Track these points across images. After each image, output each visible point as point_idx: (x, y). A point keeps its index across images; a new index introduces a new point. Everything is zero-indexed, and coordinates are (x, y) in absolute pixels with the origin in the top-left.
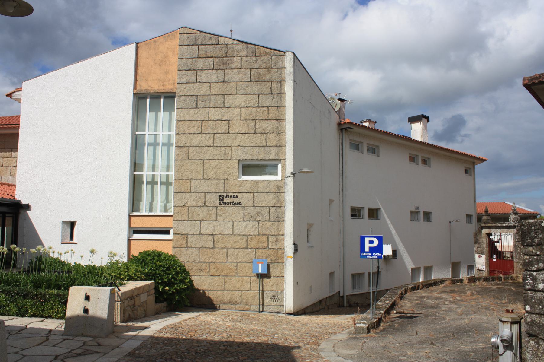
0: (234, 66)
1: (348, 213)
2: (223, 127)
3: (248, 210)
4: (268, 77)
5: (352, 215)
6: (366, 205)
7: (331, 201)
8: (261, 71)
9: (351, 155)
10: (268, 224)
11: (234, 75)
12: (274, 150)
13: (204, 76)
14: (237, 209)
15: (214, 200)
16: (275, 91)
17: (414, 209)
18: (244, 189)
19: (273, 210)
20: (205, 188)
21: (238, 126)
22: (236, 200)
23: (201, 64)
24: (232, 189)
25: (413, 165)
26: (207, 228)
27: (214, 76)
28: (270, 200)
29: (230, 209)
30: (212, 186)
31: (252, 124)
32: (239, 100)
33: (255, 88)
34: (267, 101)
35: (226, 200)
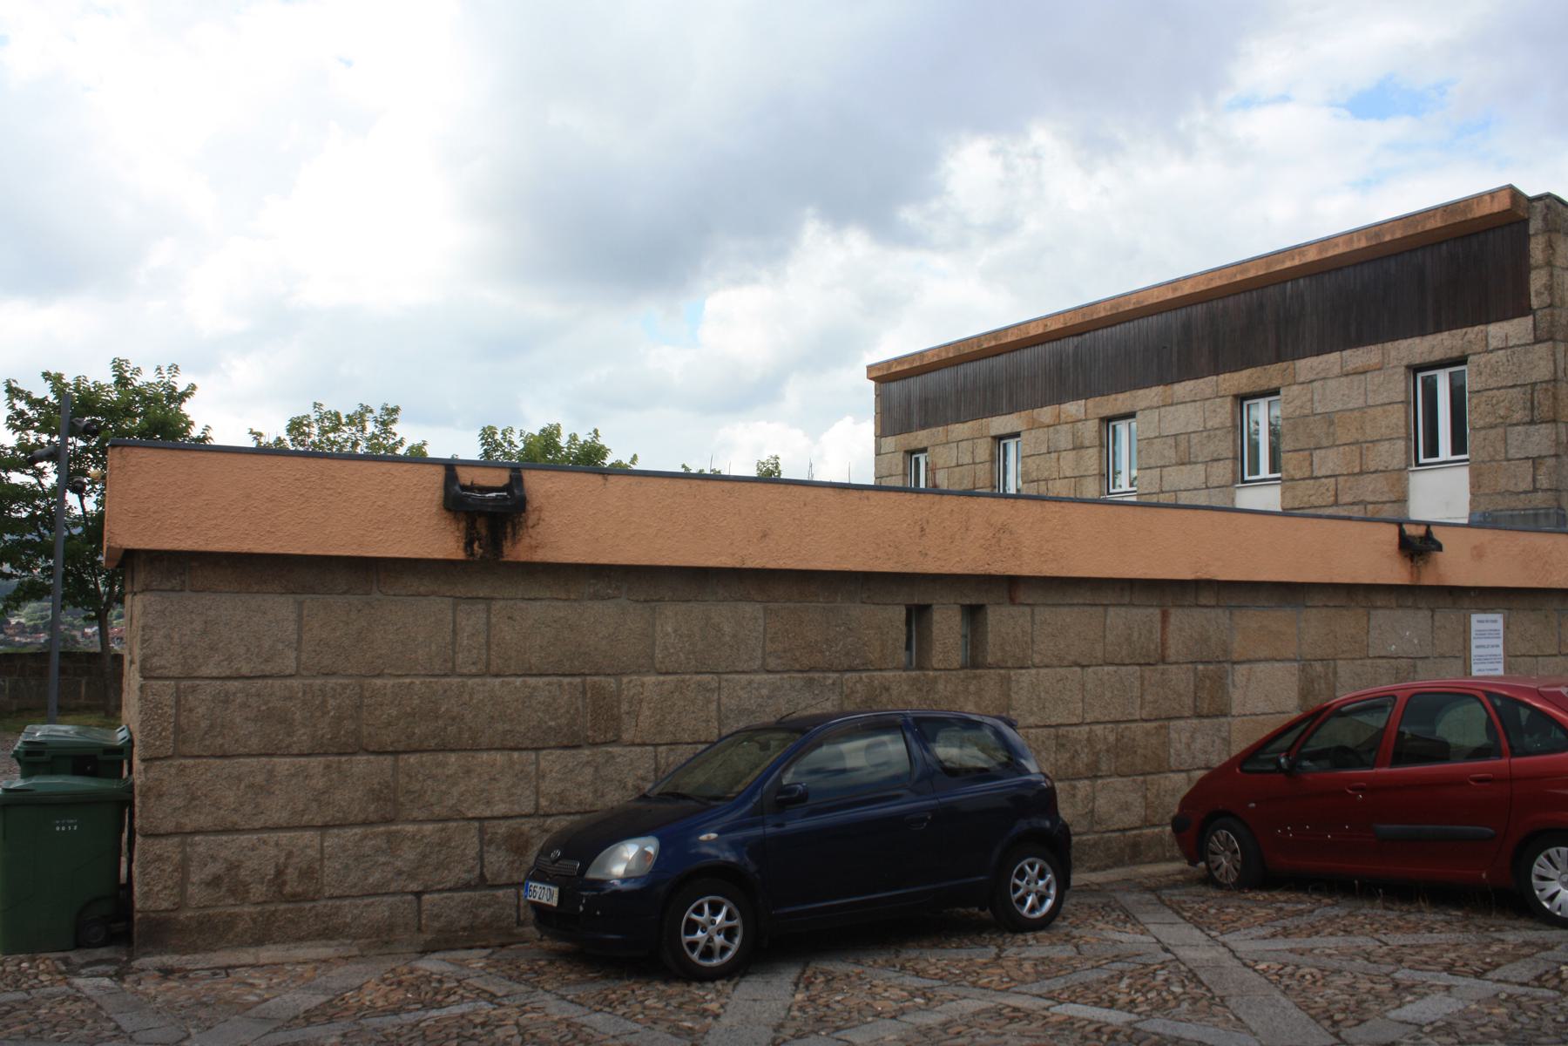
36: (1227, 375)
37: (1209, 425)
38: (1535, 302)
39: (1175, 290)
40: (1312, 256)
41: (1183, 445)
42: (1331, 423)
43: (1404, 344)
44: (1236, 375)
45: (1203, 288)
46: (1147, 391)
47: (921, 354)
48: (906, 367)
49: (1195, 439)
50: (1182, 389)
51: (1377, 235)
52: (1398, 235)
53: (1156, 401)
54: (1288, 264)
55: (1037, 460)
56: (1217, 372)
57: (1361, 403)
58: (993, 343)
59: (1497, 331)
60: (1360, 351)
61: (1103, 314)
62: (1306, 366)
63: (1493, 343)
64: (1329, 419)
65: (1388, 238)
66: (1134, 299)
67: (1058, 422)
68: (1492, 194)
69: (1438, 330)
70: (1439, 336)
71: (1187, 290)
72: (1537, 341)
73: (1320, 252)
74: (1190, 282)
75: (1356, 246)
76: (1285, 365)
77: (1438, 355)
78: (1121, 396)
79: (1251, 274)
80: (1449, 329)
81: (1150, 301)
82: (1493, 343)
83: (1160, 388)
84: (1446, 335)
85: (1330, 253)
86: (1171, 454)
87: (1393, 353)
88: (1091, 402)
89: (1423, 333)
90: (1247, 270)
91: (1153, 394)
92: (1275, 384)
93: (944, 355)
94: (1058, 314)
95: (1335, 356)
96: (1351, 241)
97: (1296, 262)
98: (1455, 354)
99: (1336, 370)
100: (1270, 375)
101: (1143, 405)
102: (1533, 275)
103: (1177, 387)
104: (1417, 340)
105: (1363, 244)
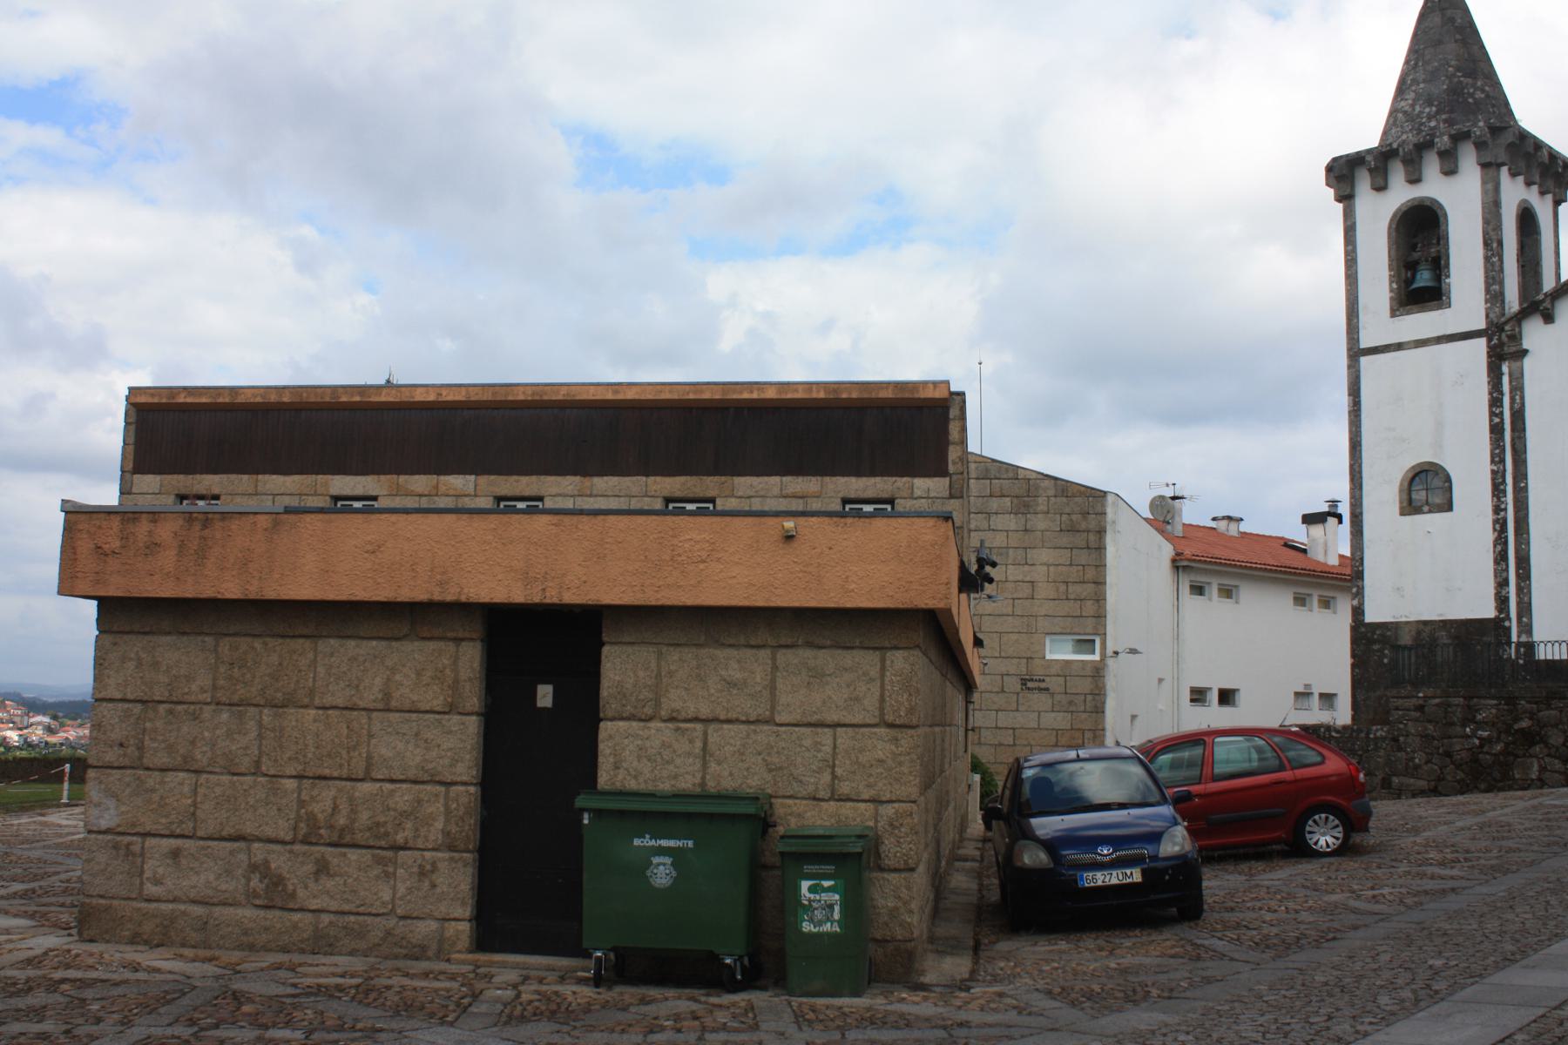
0: (1040, 508)
1: (1187, 695)
2: (1025, 590)
3: (1057, 698)
4: (1083, 526)
5: (1192, 700)
6: (1216, 684)
7: (1160, 680)
8: (1074, 517)
9: (1191, 602)
10: (1084, 716)
11: (1040, 523)
12: (1090, 621)
13: (999, 522)
14: (1044, 697)
15: (1013, 684)
16: (1092, 545)
17: (1301, 689)
18: (1053, 671)
19: (1089, 698)
20: (1004, 670)
21: (1044, 590)
22: (1043, 685)
23: (994, 504)
24: (1039, 671)
25: (1301, 612)
26: (1004, 720)
27: (1012, 522)
28: (1085, 685)
29: (1036, 696)
30: (1010, 667)
31: (1063, 588)
32: (1045, 555)
33: (1065, 540)
34: (1083, 557)
35: (1030, 684)
36: (658, 479)
38: (951, 469)
39: (616, 392)
40: (771, 394)
43: (841, 480)
45: (650, 397)
46: (559, 479)
47: (234, 390)
48: (204, 400)
51: (835, 391)
52: (854, 395)
53: (570, 489)
54: (746, 396)
58: (357, 399)
59: (921, 484)
60: (800, 479)
61: (521, 397)
63: (918, 493)
65: (844, 396)
66: (564, 391)
68: (935, 384)
69: (873, 474)
70: (873, 480)
71: (630, 395)
72: (951, 497)
73: (779, 392)
74: (634, 389)
75: (815, 395)
76: (723, 478)
77: (870, 494)
78: (524, 479)
79: (707, 396)
80: (882, 475)
81: (584, 397)
82: (918, 493)
84: (878, 479)
85: (789, 396)
87: (831, 486)
88: (483, 479)
89: (858, 474)
90: (702, 392)
92: (710, 494)
93: (273, 398)
94: (460, 386)
95: (775, 480)
96: (810, 390)
97: (755, 396)
98: (885, 495)
99: (776, 491)
101: (554, 490)
102: (951, 448)
103: (596, 480)
104: (853, 479)
105: (822, 395)
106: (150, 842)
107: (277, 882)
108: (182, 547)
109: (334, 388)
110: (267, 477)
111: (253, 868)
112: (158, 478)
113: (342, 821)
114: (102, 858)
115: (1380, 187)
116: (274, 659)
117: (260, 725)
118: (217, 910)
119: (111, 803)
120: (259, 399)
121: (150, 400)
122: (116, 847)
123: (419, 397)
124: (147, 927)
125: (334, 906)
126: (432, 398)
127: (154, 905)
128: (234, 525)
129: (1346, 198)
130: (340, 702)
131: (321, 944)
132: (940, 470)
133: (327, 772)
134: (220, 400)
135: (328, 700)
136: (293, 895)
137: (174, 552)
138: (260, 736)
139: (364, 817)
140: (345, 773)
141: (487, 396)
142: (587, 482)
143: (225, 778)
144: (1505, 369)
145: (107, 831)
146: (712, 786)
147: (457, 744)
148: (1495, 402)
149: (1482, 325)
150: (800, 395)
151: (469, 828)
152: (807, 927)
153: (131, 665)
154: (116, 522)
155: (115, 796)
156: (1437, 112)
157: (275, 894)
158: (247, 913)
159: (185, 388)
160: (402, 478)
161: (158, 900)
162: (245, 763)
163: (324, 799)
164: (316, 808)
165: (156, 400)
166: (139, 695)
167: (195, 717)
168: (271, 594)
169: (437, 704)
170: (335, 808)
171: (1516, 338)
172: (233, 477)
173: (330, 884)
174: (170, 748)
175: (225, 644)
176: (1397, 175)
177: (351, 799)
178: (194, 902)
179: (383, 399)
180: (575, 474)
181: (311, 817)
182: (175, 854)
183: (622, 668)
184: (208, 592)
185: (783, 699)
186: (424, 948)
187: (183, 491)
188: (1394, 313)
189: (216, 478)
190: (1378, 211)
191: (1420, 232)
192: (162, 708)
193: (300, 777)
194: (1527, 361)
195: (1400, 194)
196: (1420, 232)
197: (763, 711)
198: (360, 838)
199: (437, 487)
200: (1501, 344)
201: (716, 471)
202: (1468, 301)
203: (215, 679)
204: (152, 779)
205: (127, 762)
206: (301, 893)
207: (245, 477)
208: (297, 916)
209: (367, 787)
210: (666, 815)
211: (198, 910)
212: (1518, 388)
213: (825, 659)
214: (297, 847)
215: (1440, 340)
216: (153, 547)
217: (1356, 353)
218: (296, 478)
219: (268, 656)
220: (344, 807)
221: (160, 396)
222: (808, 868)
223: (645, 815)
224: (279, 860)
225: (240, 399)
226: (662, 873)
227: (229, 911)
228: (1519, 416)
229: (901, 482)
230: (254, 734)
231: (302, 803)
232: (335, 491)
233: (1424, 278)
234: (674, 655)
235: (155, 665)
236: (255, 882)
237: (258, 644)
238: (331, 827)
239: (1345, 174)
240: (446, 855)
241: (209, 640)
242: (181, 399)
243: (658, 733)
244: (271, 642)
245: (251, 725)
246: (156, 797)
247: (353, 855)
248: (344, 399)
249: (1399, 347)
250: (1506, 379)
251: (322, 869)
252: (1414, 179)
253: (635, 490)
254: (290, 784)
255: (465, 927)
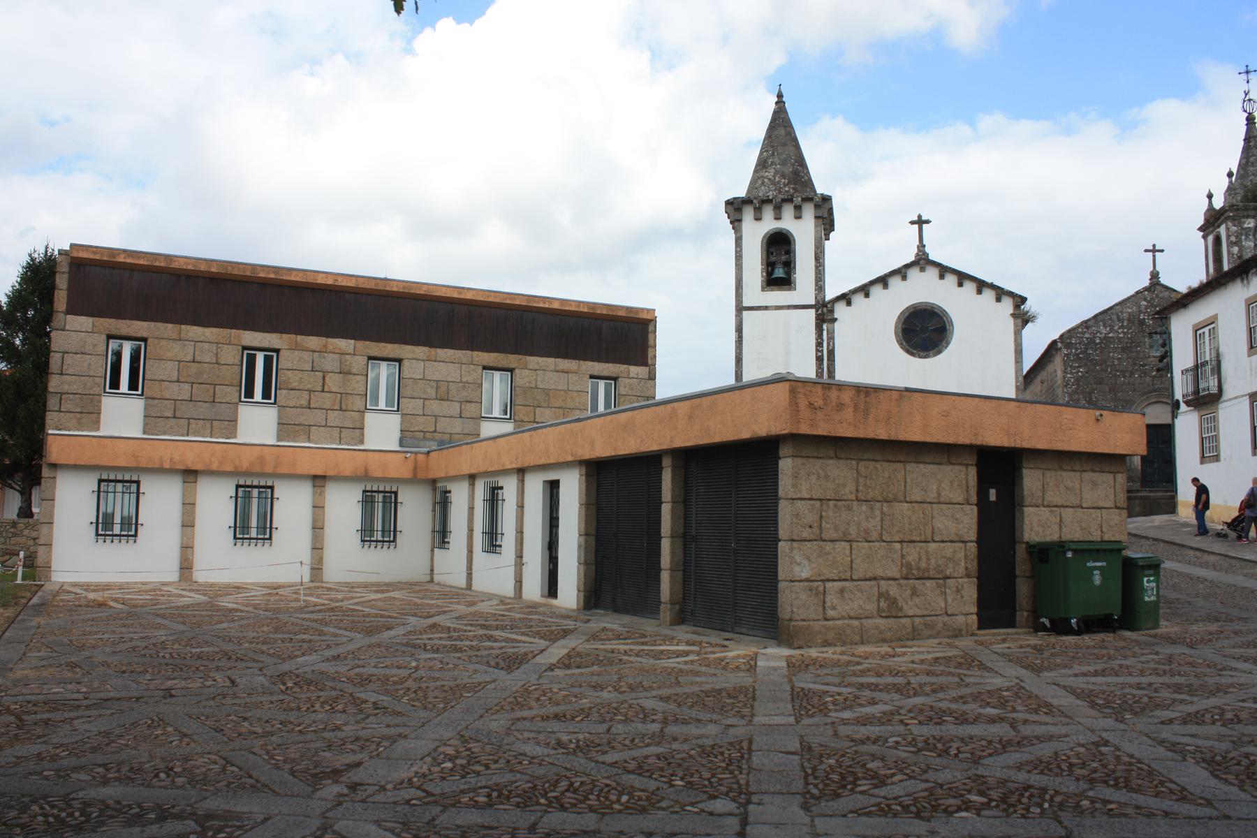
37: (464, 380)
40: (556, 306)
41: (443, 389)
42: (548, 394)
43: (590, 363)
44: (486, 355)
47: (168, 257)
48: (142, 262)
49: (452, 386)
50: (442, 353)
53: (421, 356)
54: (541, 305)
55: (300, 374)
56: (472, 348)
57: (565, 387)
58: (273, 276)
59: (634, 370)
62: (533, 361)
63: (632, 375)
64: (546, 392)
66: (425, 288)
67: (323, 351)
69: (607, 362)
71: (469, 296)
77: (605, 374)
78: (390, 346)
82: (632, 375)
83: (426, 349)
86: (432, 392)
88: (360, 344)
89: (599, 361)
91: (421, 351)
92: (512, 366)
93: (203, 267)
95: (551, 360)
97: (547, 306)
99: (552, 367)
100: (511, 360)
101: (410, 355)
103: (439, 350)
105: (586, 310)
106: (829, 585)
107: (893, 602)
108: (856, 407)
109: (254, 266)
110: (189, 327)
111: (880, 595)
112: (90, 320)
113: (923, 565)
114: (803, 596)
115: (758, 218)
116: (886, 474)
117: (882, 513)
118: (864, 621)
119: (806, 562)
120: (190, 267)
121: (92, 256)
122: (811, 590)
123: (320, 280)
124: (830, 636)
125: (919, 612)
126: (330, 282)
127: (831, 623)
128: (882, 395)
129: (736, 222)
130: (919, 499)
131: (915, 635)
132: (645, 364)
133: (914, 538)
134: (157, 264)
135: (914, 498)
136: (901, 609)
137: (851, 410)
138: (882, 520)
139: (933, 561)
140: (923, 538)
141: (371, 286)
142: (433, 351)
143: (866, 544)
144: (825, 327)
145: (807, 580)
146: (1106, 538)
147: (966, 521)
148: (819, 344)
149: (813, 303)
150: (573, 308)
151: (973, 566)
152: (1147, 599)
153: (814, 477)
154: (819, 389)
155: (809, 559)
156: (789, 183)
157: (892, 609)
158: (880, 622)
159: (125, 251)
160: (299, 338)
161: (834, 619)
162: (874, 536)
163: (913, 553)
164: (910, 558)
165: (98, 257)
166: (819, 495)
167: (849, 509)
168: (901, 438)
169: (960, 499)
170: (920, 558)
171: (832, 311)
172: (159, 324)
173: (917, 600)
174: (836, 528)
175: (862, 464)
176: (768, 212)
177: (927, 553)
178: (850, 618)
179: (293, 278)
180: (425, 345)
181: (909, 565)
182: (842, 591)
183: (1031, 480)
184: (871, 435)
185: (1085, 496)
186: (960, 630)
187: (114, 332)
188: (763, 290)
189: (145, 324)
190: (756, 231)
191: (779, 247)
192: (831, 503)
193: (901, 542)
194: (836, 324)
195: (769, 224)
196: (779, 247)
197: (1076, 502)
198: (932, 573)
199: (325, 346)
200: (823, 314)
201: (516, 351)
202: (804, 290)
203: (857, 485)
204: (828, 547)
205: (812, 537)
206: (905, 607)
207: (170, 326)
208: (903, 620)
209: (933, 545)
210: (1098, 551)
211: (856, 623)
212: (831, 338)
213: (1098, 477)
214: (902, 582)
215: (789, 307)
216: (840, 406)
217: (740, 309)
218: (214, 330)
219: (883, 472)
220: (924, 557)
221: (102, 254)
222: (1147, 572)
223: (1090, 551)
224: (894, 590)
225: (175, 265)
226: (1097, 579)
227: (870, 621)
228: (831, 353)
229: (623, 367)
230: (879, 518)
231: (903, 556)
232: (246, 343)
233: (779, 273)
234: (1048, 474)
235: (827, 477)
236: (883, 604)
237: (878, 465)
238: (919, 569)
239: (735, 208)
240: (966, 580)
241: (854, 463)
242: (121, 259)
243: (1045, 512)
244: (886, 465)
245: (878, 513)
246: (830, 557)
247: (929, 583)
248: (262, 275)
249: (766, 308)
250: (825, 333)
251: (914, 592)
252: (778, 218)
253: (464, 360)
254: (898, 546)
255: (975, 617)
